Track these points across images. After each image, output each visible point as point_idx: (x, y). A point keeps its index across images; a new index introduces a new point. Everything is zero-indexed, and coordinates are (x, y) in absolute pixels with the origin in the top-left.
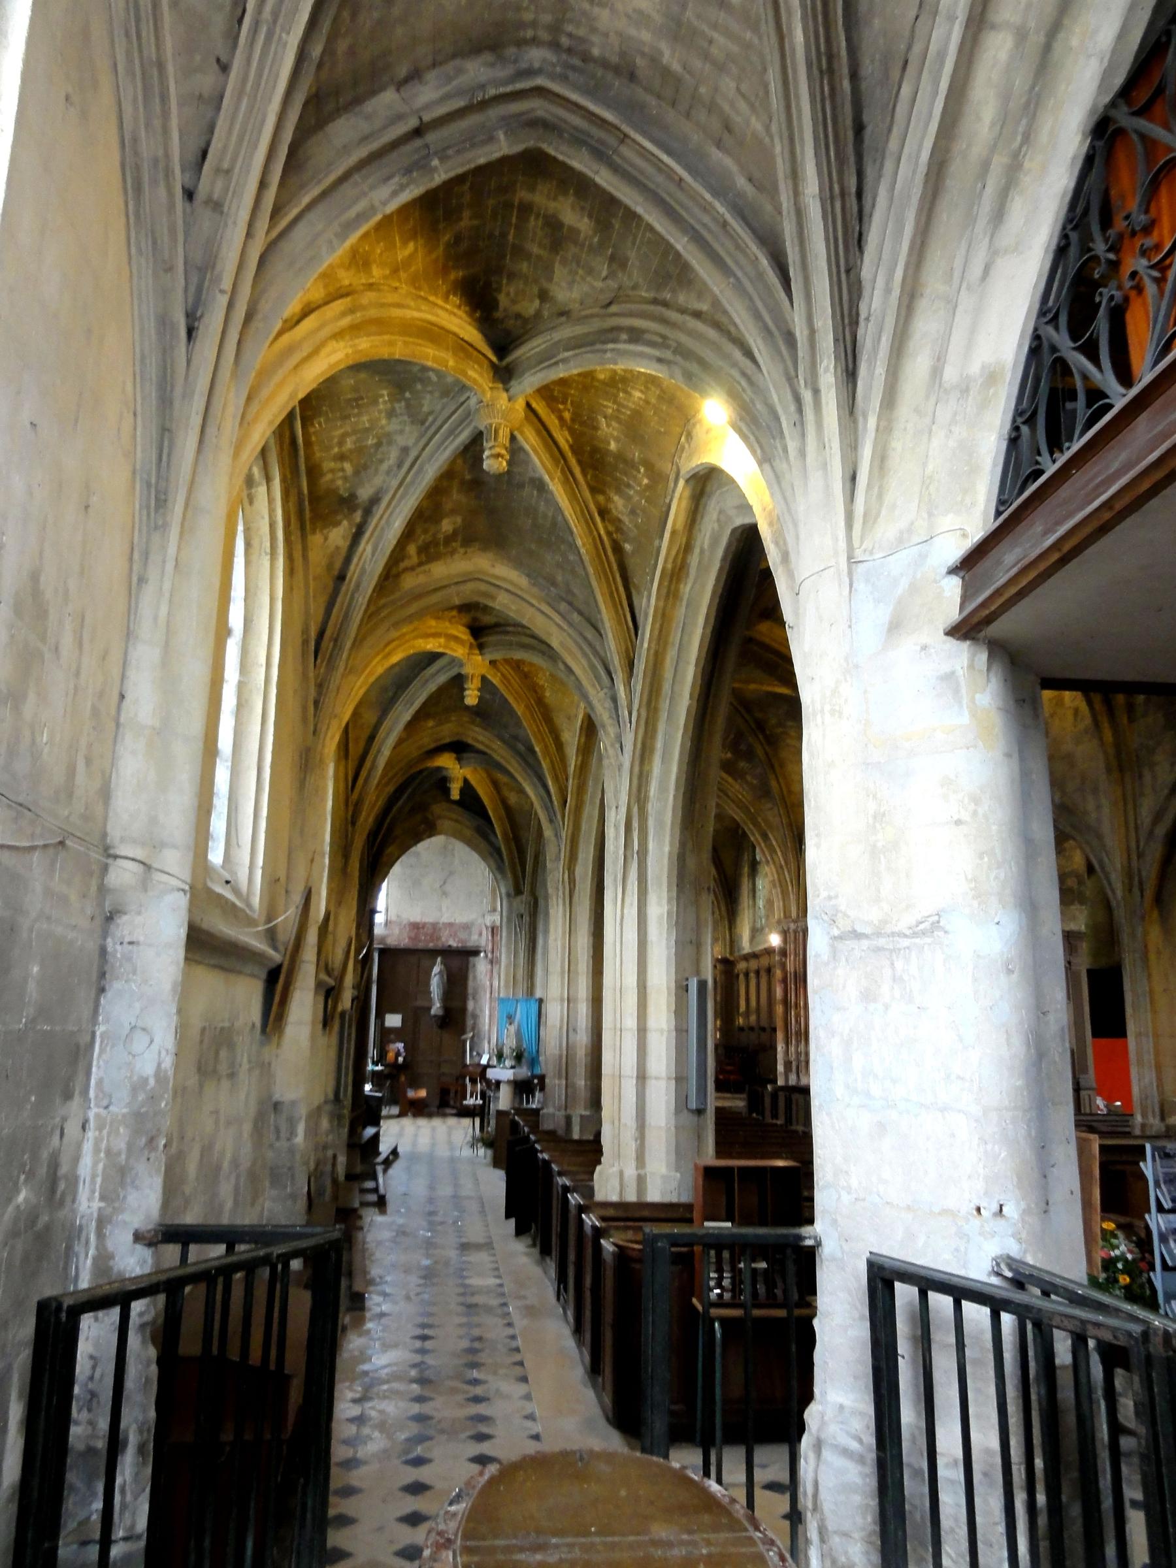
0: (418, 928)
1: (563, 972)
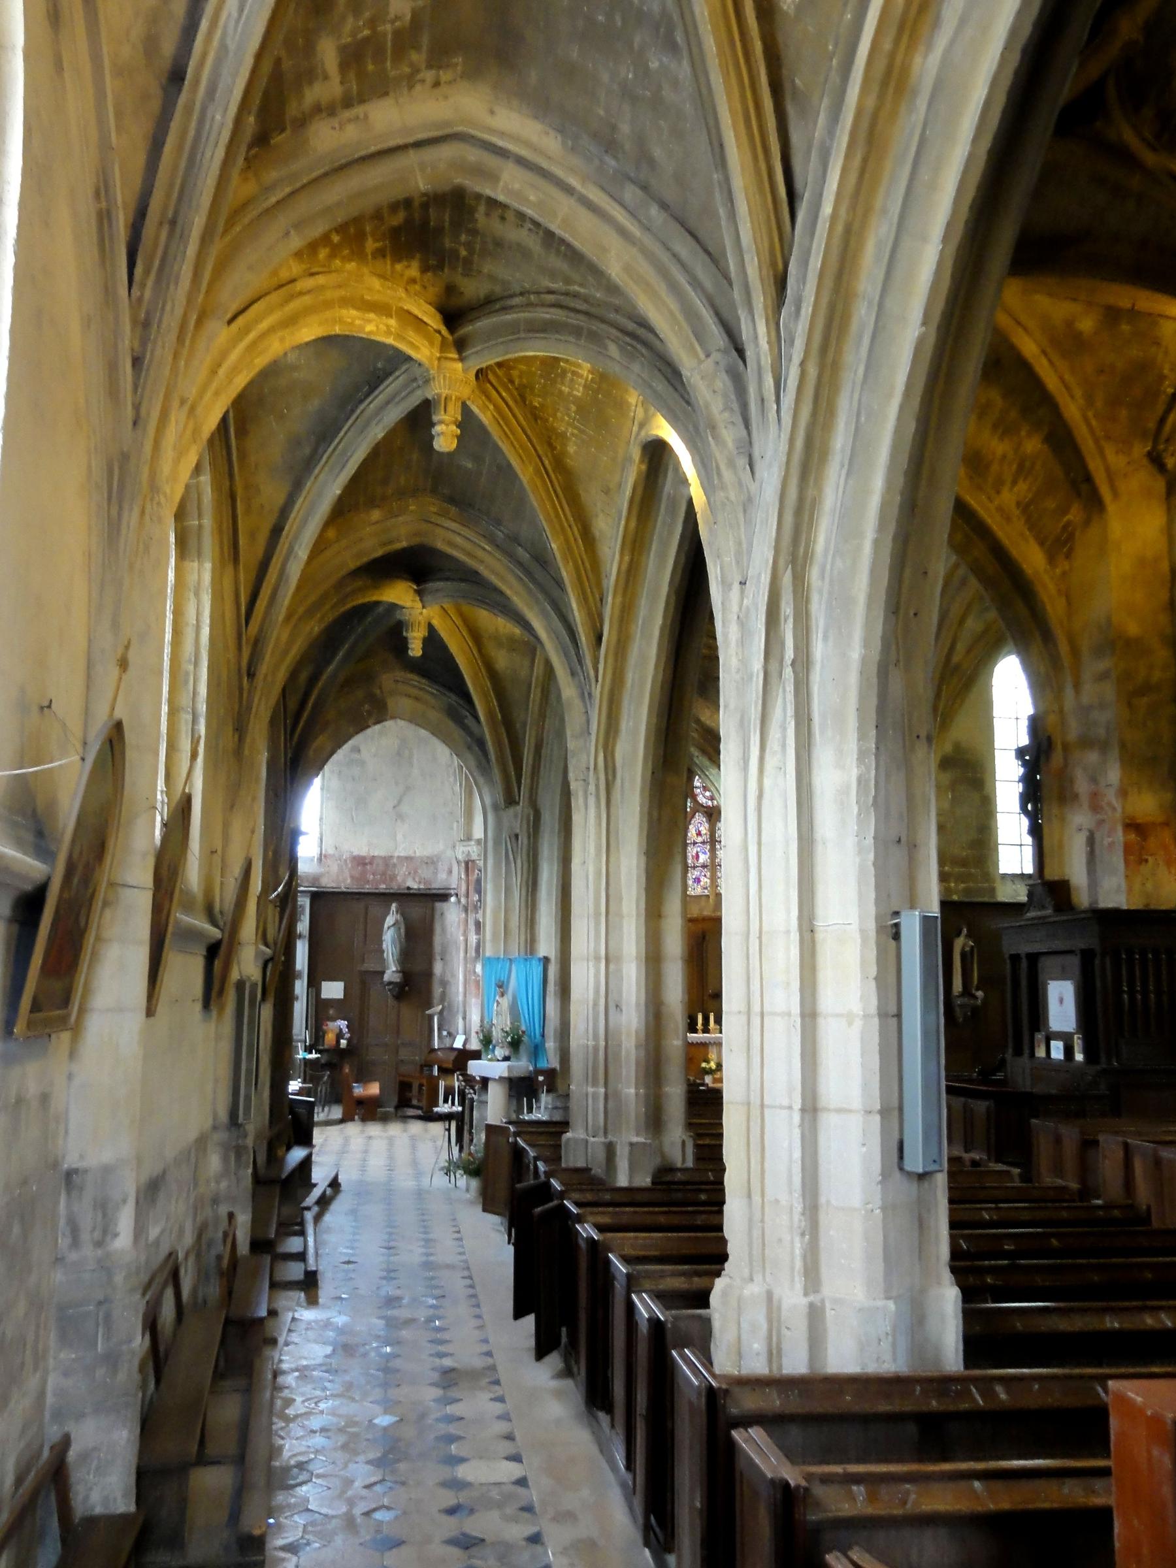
1: (597, 914)
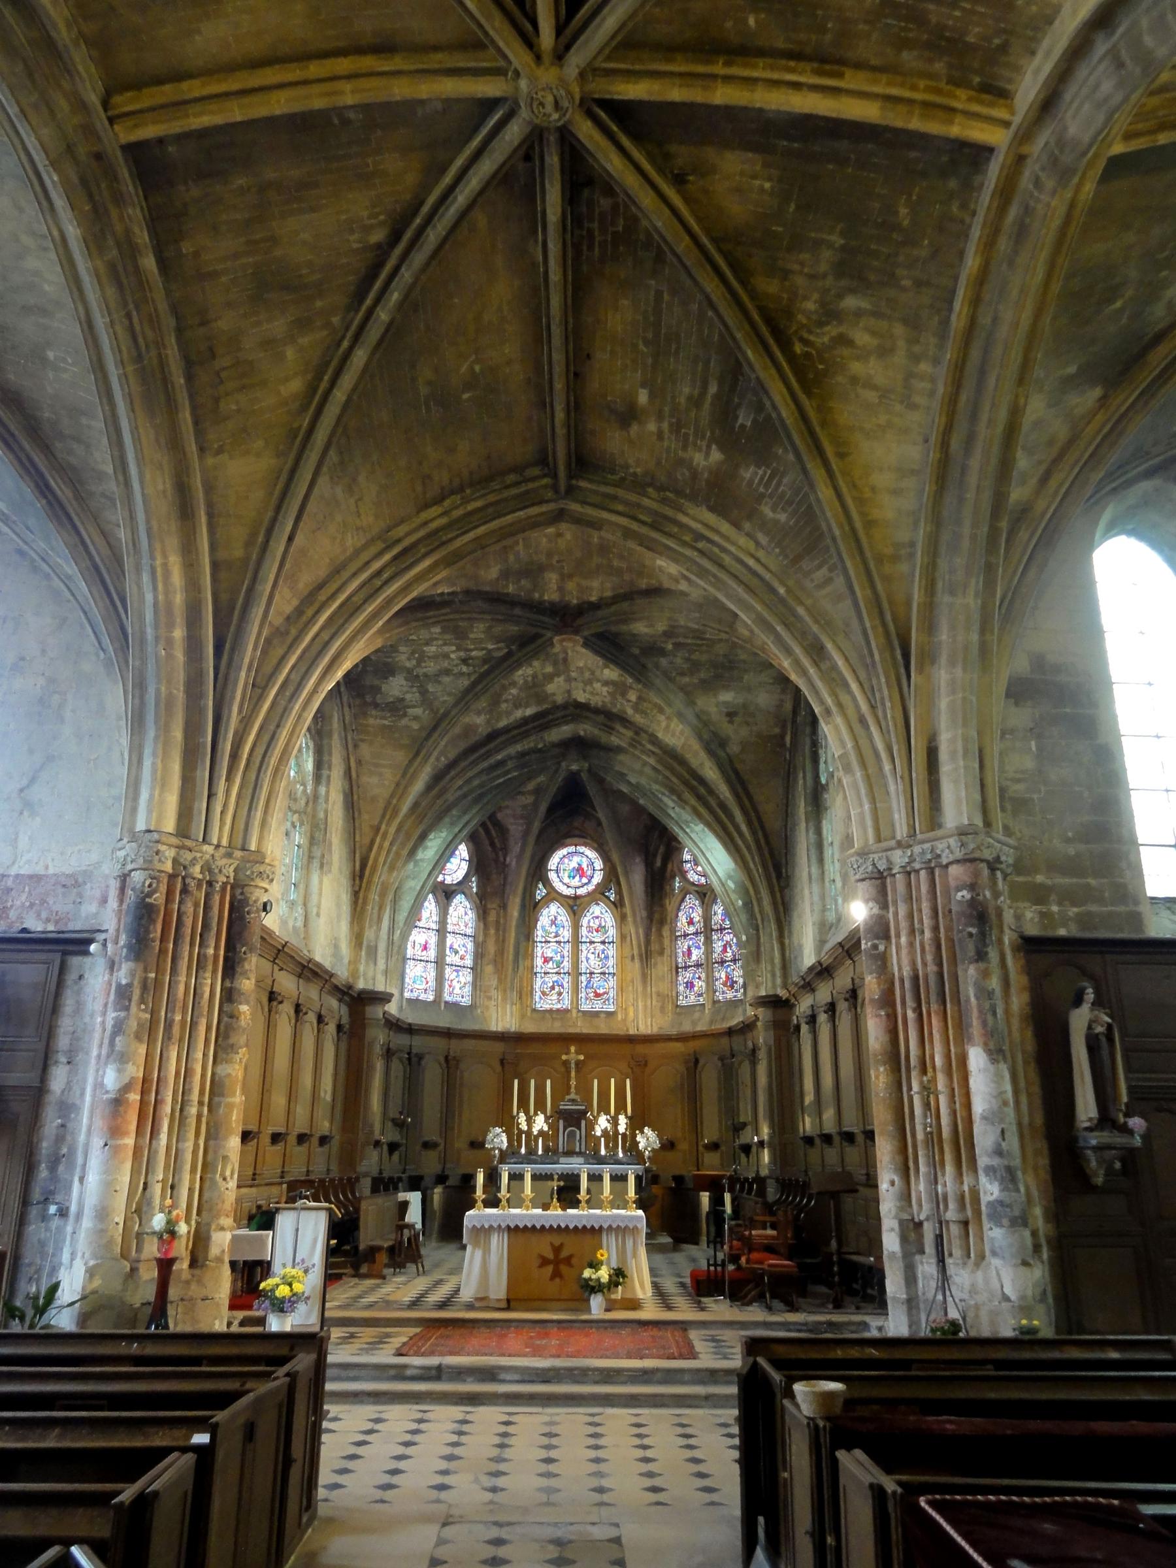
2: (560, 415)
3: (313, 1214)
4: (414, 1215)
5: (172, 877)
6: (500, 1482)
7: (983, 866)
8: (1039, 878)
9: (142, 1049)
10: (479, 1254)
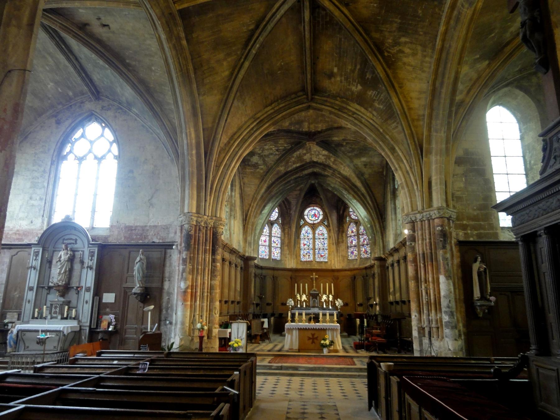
0: (132, 230)
2: (309, 76)
3: (242, 324)
4: (266, 325)
5: (196, 226)
6: (303, 393)
7: (446, 219)
8: (465, 222)
9: (191, 277)
10: (290, 336)
